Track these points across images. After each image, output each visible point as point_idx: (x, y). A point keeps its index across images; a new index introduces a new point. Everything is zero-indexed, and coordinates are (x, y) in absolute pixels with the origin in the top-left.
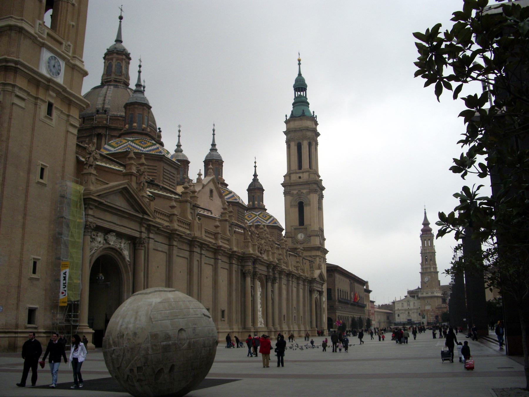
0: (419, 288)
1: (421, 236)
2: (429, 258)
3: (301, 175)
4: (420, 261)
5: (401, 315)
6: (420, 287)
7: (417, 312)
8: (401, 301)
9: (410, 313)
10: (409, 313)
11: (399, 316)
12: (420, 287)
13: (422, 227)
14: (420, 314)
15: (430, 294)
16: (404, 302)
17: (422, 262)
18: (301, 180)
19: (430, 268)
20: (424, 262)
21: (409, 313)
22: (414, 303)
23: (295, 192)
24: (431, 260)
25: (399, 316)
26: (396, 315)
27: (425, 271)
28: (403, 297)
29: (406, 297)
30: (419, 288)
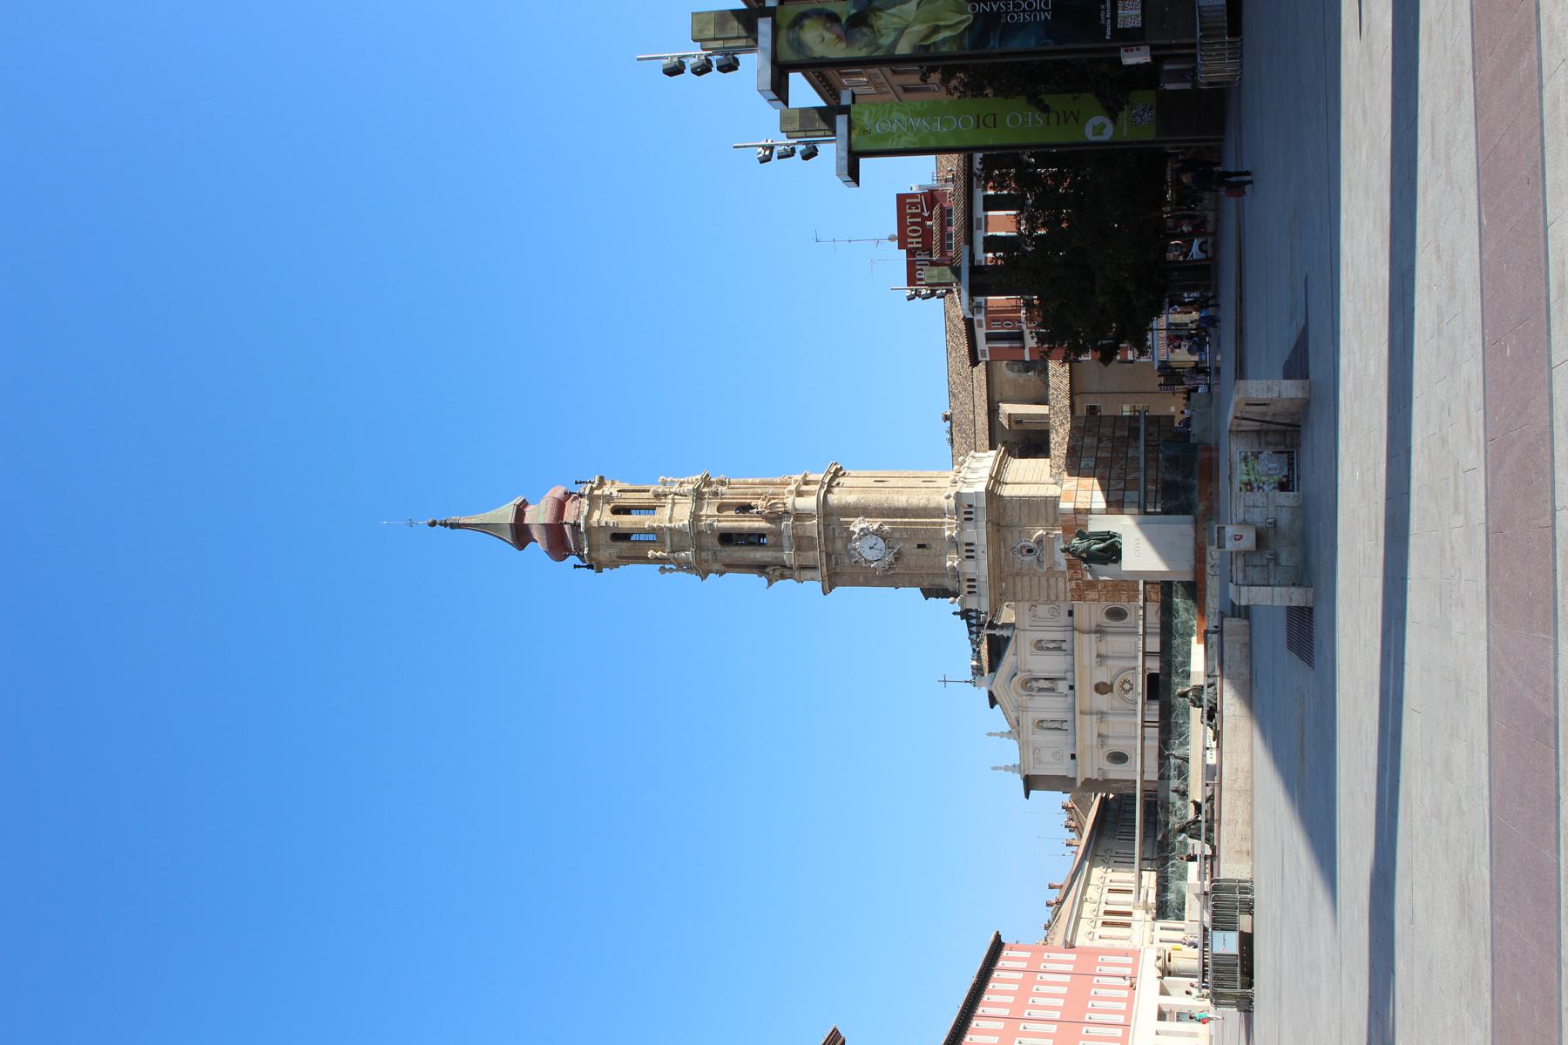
1: (594, 565)
2: (732, 522)
4: (755, 581)
5: (1115, 745)
7: (1100, 631)
8: (1016, 730)
9: (1103, 676)
10: (1102, 688)
11: (1119, 758)
14: (1117, 614)
15: (978, 534)
16: (1028, 720)
17: (760, 568)
19: (800, 516)
21: (1102, 688)
22: (1039, 646)
24: (745, 508)
25: (1119, 758)
26: (1116, 772)
27: (815, 556)
28: (997, 719)
29: (993, 702)
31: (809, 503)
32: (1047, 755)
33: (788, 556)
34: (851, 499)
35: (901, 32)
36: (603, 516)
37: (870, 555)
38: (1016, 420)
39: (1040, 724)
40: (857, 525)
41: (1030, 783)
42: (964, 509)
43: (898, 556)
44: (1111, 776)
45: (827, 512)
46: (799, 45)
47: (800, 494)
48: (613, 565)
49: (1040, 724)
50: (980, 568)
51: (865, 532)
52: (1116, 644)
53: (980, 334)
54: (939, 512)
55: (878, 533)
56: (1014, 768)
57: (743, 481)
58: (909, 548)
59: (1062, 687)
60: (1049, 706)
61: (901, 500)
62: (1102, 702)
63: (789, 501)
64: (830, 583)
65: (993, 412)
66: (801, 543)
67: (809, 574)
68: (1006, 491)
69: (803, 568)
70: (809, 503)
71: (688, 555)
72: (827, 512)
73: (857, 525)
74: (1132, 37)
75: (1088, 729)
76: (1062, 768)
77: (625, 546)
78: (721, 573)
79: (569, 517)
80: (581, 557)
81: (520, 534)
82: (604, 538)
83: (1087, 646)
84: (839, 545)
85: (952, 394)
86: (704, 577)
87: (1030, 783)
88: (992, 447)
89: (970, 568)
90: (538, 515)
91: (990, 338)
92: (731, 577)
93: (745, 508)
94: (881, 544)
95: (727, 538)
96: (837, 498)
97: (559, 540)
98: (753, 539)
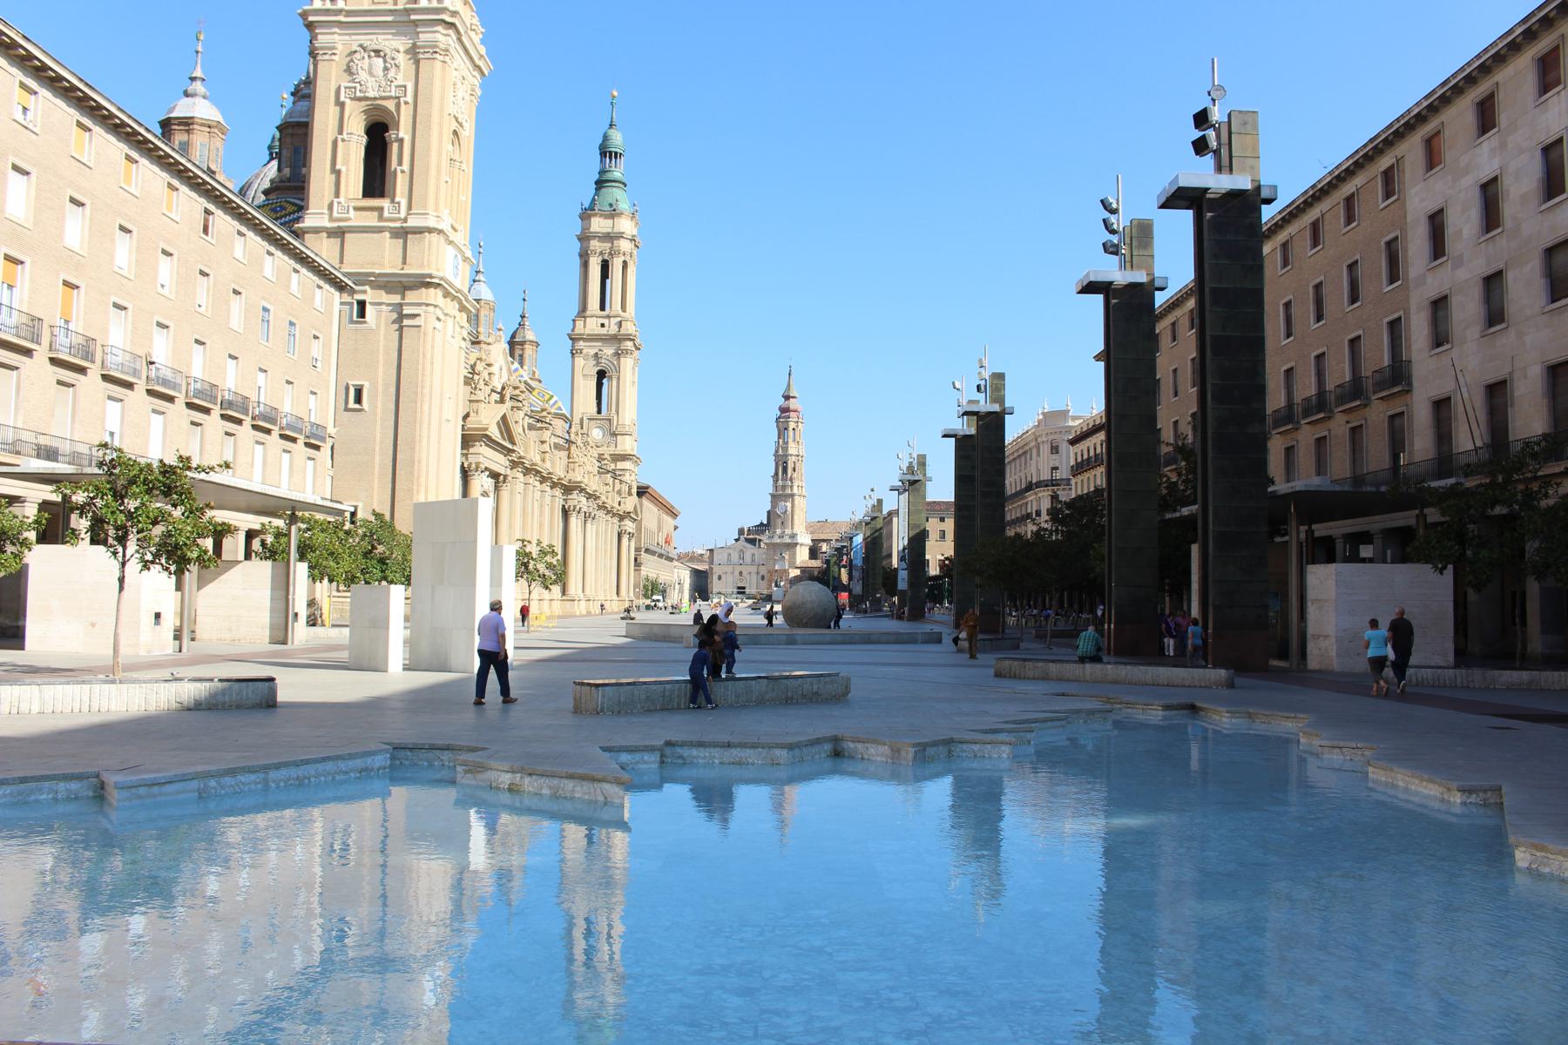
2: (790, 466)
3: (606, 321)
15: (787, 540)
17: (776, 474)
18: (604, 331)
23: (593, 352)
26: (715, 577)
36: (792, 425)
40: (789, 505)
41: (711, 551)
42: (793, 536)
45: (792, 496)
57: (801, 467)
60: (735, 557)
64: (773, 496)
66: (784, 487)
70: (795, 490)
72: (792, 496)
73: (789, 505)
75: (729, 569)
77: (782, 429)
81: (787, 398)
83: (754, 569)
90: (792, 404)
97: (784, 410)
98: (785, 470)
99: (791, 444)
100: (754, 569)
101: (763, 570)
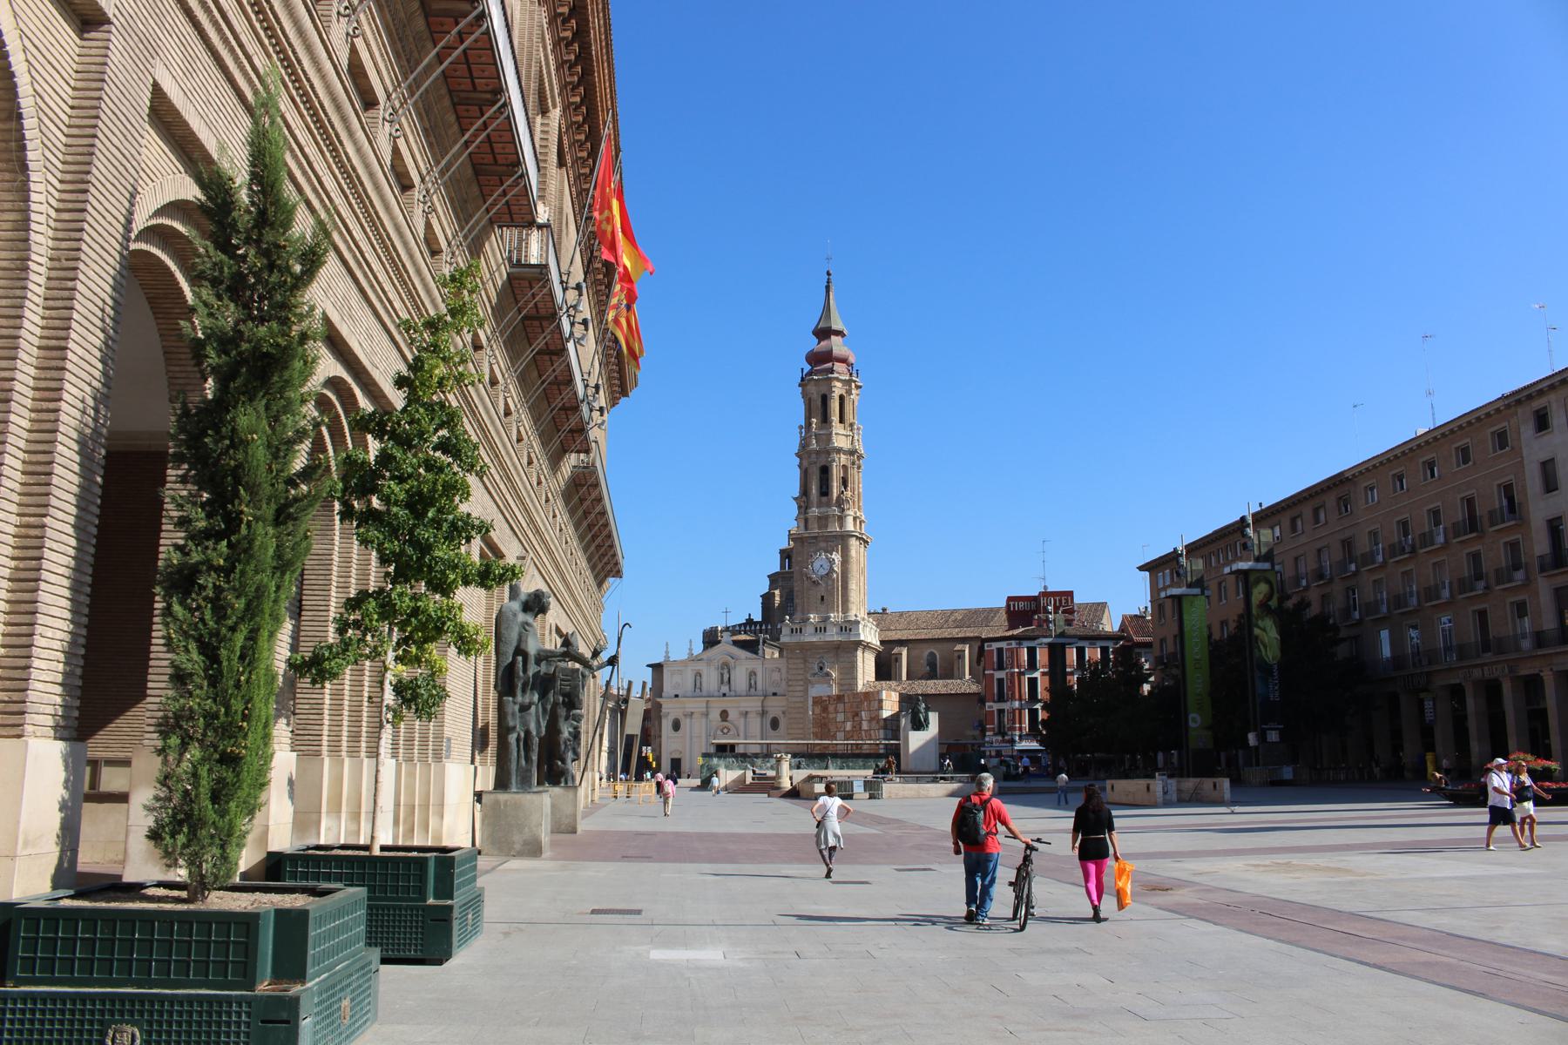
0: (750, 622)
1: (804, 382)
5: (685, 723)
6: (757, 617)
7: (763, 713)
8: (693, 659)
9: (733, 715)
10: (724, 715)
11: (676, 726)
12: (757, 617)
13: (812, 344)
14: (775, 724)
15: (833, 635)
16: (702, 667)
17: (805, 491)
19: (841, 519)
20: (814, 490)
21: (724, 715)
22: (752, 674)
24: (845, 482)
25: (676, 726)
26: (666, 725)
27: (815, 530)
30: (750, 622)
31: (850, 525)
32: (677, 679)
33: (814, 511)
34: (853, 553)
35: (1264, 630)
36: (838, 389)
37: (817, 565)
38: (898, 658)
39: (699, 674)
40: (837, 557)
41: (657, 668)
42: (849, 626)
43: (815, 583)
44: (664, 722)
45: (844, 538)
46: (1257, 582)
47: (855, 519)
48: (804, 394)
49: (699, 674)
50: (809, 637)
51: (832, 562)
52: (755, 724)
53: (1003, 645)
54: (845, 610)
55: (832, 570)
56: (667, 657)
58: (822, 590)
59: (725, 689)
60: (711, 680)
61: (853, 586)
62: (715, 715)
63: (851, 512)
65: (901, 643)
66: (823, 520)
67: (802, 525)
68: (859, 653)
69: (806, 521)
70: (850, 525)
71: (814, 445)
72: (844, 538)
73: (836, 557)
74: (1262, 737)
75: (697, 705)
76: (668, 688)
78: (800, 466)
79: (838, 367)
80: (810, 373)
81: (823, 333)
82: (824, 390)
83: (753, 704)
84: (823, 545)
85: (901, 614)
86: (797, 455)
87: (657, 668)
88: (882, 642)
89: (810, 629)
90: (837, 345)
91: (1000, 650)
92: (797, 472)
93: (845, 482)
94: (823, 572)
95: (825, 471)
96: (853, 542)
97: (821, 359)
99: (837, 428)
100: (753, 704)
101: (775, 707)
